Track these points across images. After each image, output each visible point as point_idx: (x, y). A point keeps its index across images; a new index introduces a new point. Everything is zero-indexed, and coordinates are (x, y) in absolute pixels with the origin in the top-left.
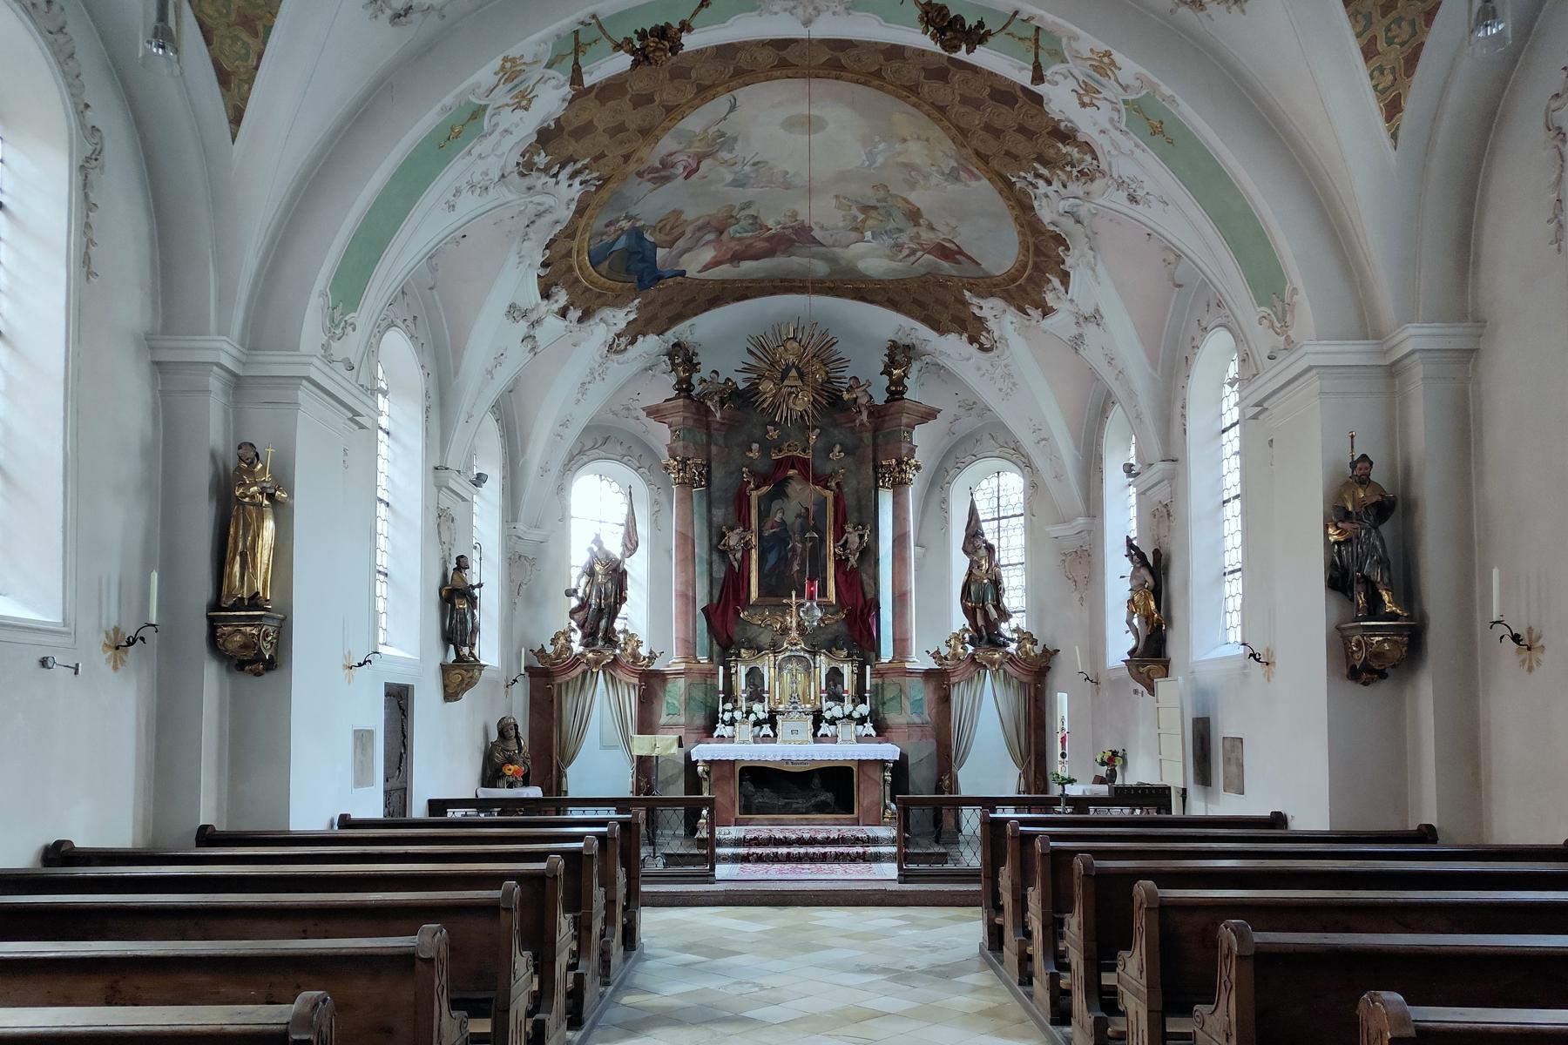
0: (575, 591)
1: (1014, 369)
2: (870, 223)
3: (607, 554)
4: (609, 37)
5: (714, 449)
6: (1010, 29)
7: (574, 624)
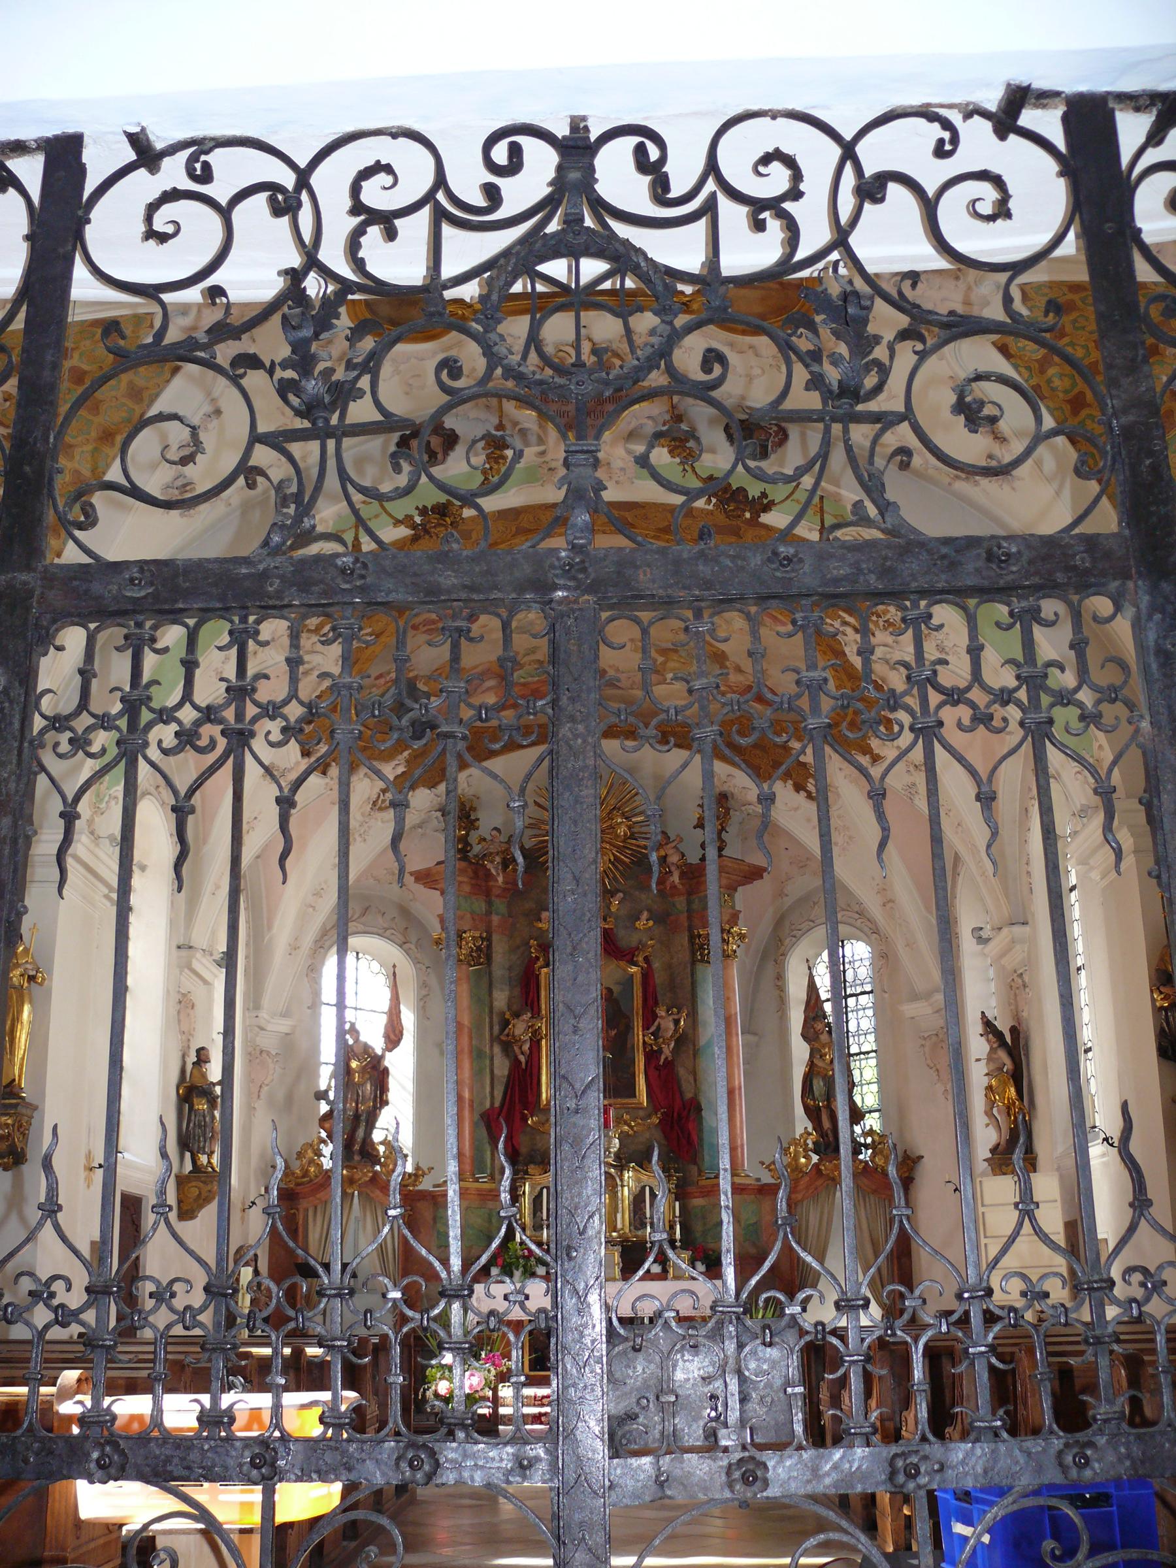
0: (326, 1092)
1: (844, 822)
2: (671, 665)
3: (367, 1048)
4: (390, 515)
5: (495, 919)
6: (794, 496)
7: (324, 1134)
